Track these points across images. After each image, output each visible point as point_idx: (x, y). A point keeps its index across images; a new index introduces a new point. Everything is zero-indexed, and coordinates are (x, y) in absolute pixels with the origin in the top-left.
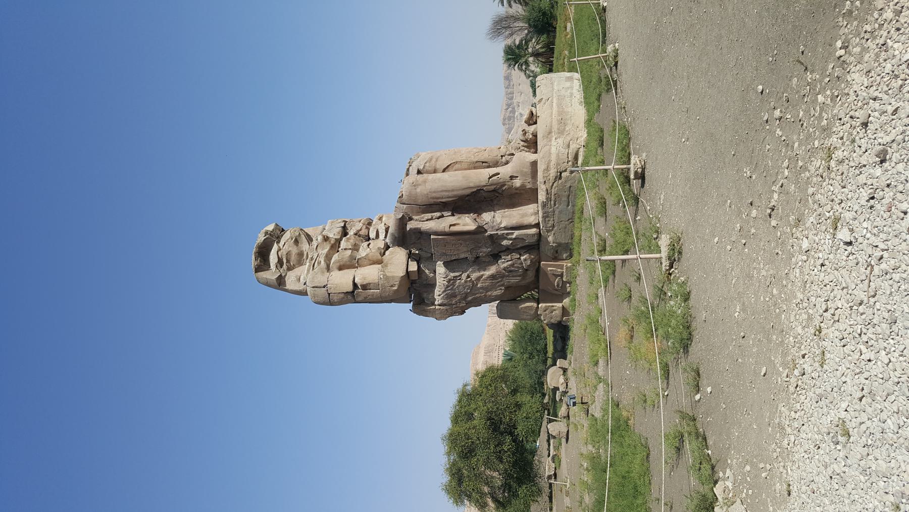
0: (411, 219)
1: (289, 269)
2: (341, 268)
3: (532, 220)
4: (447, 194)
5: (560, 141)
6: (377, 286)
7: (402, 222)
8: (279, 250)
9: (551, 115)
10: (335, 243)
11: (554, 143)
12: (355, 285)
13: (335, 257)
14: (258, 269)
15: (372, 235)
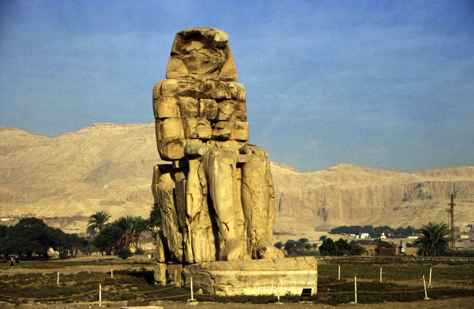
0: (201, 161)
1: (183, 60)
2: (179, 104)
3: (198, 257)
4: (213, 190)
5: (234, 278)
6: (162, 136)
7: (196, 156)
8: (197, 51)
9: (253, 270)
10: (205, 95)
11: (233, 273)
12: (163, 119)
13: (186, 100)
14: (181, 35)
15: (218, 125)
